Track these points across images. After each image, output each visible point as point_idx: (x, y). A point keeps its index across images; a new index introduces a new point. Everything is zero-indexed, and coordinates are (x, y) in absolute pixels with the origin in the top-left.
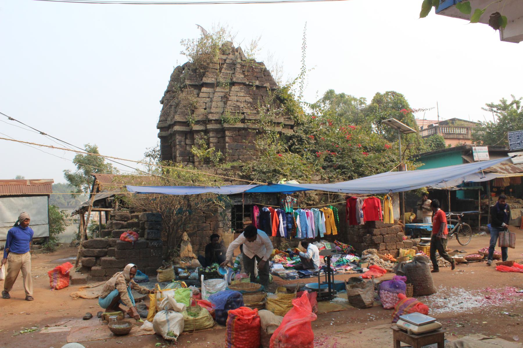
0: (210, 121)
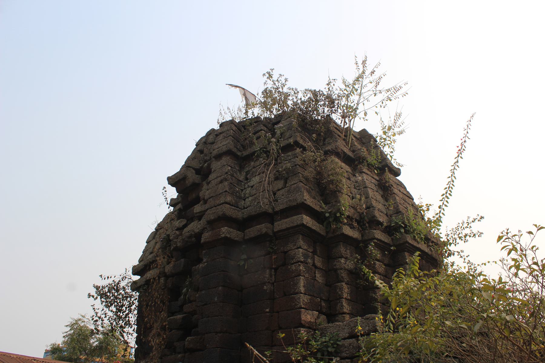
0: (375, 223)
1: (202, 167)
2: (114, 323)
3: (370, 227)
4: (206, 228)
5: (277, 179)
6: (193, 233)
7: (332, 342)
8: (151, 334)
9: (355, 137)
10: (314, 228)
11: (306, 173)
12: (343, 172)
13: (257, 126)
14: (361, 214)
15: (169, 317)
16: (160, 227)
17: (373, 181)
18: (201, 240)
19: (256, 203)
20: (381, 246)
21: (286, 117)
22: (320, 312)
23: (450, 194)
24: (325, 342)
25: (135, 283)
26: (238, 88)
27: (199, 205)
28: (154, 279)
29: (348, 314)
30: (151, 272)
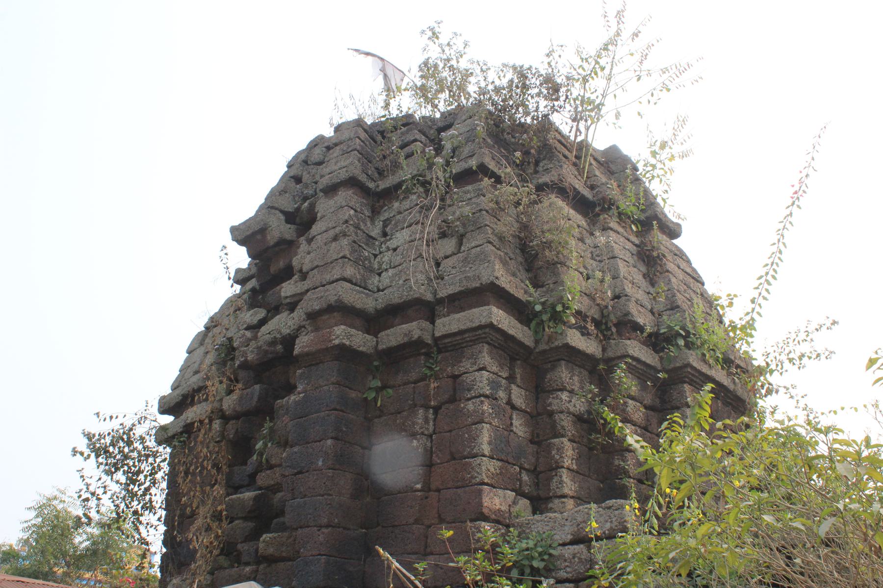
0: (628, 326)
1: (298, 209)
2: (122, 506)
3: (620, 334)
4: (304, 327)
5: (443, 235)
6: (278, 336)
7: (540, 549)
8: (193, 528)
9: (595, 159)
10: (511, 332)
11: (500, 228)
12: (571, 226)
13: (407, 132)
14: (602, 309)
15: (228, 495)
16: (213, 324)
17: (629, 246)
18: (293, 349)
19: (401, 282)
20: (641, 371)
21: (464, 118)
22: (520, 493)
23: (774, 277)
24: (527, 549)
25: (163, 428)
26: (370, 58)
27: (292, 281)
28: (201, 422)
29: (572, 497)
30: (195, 408)
